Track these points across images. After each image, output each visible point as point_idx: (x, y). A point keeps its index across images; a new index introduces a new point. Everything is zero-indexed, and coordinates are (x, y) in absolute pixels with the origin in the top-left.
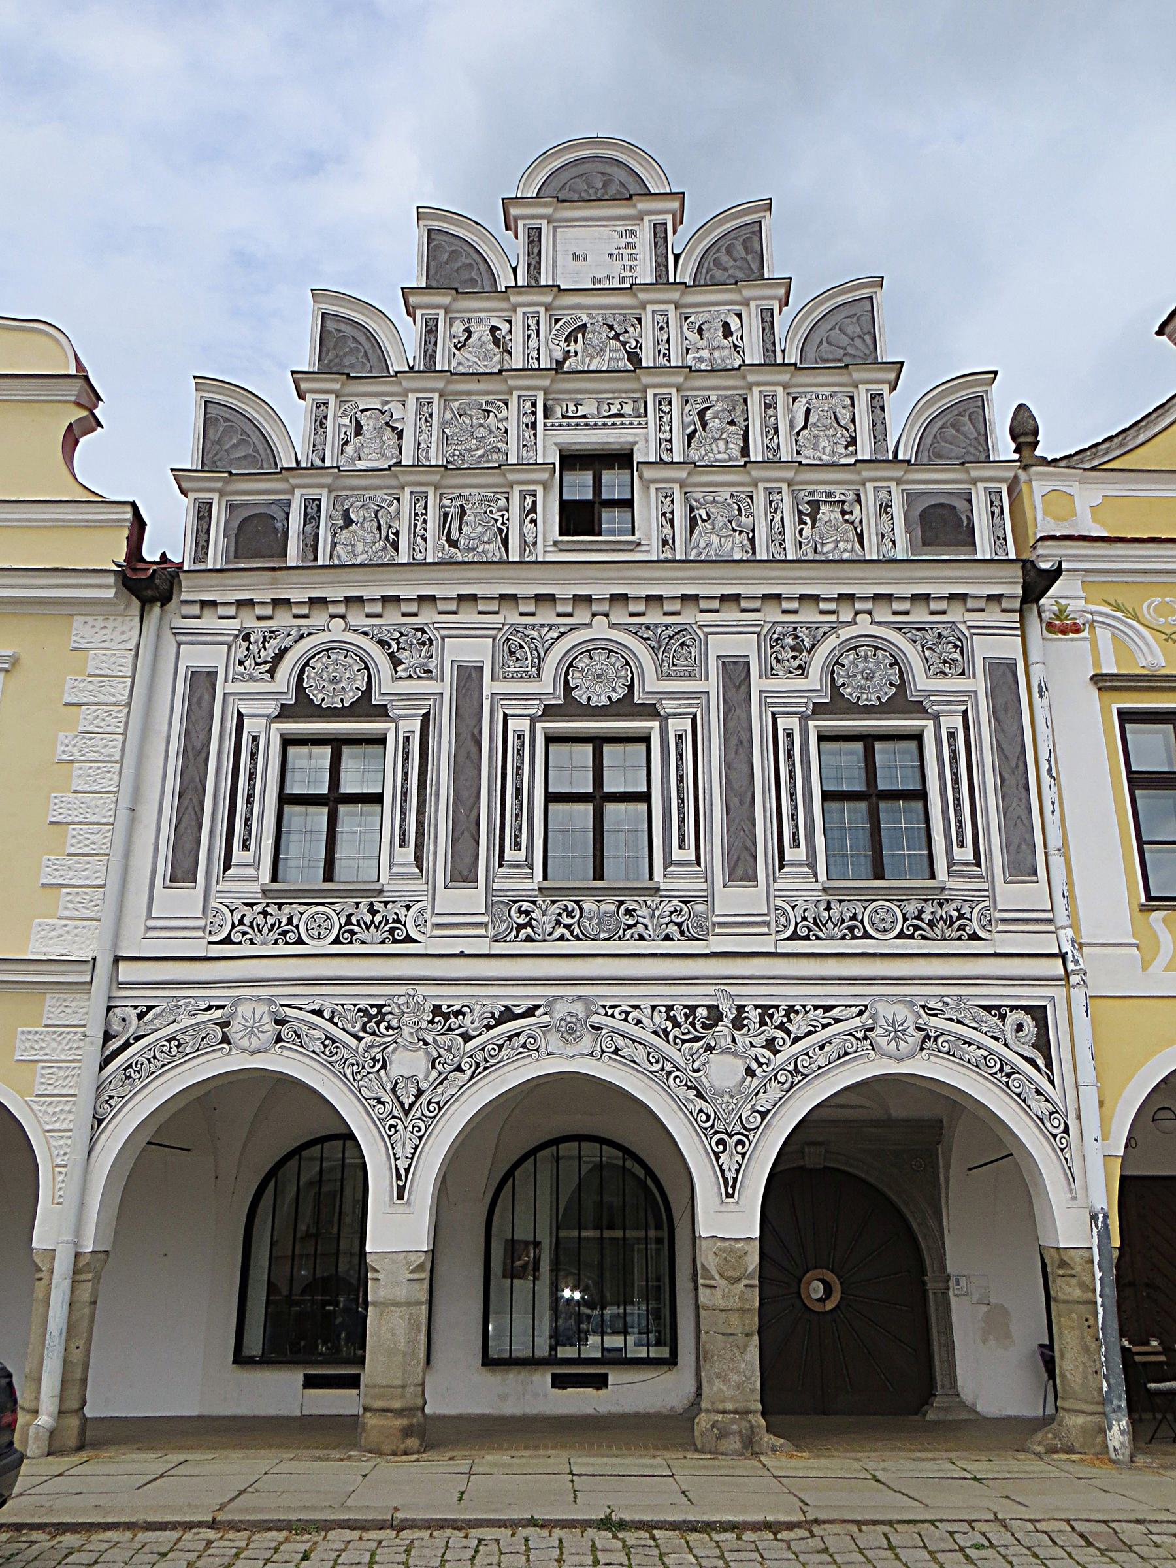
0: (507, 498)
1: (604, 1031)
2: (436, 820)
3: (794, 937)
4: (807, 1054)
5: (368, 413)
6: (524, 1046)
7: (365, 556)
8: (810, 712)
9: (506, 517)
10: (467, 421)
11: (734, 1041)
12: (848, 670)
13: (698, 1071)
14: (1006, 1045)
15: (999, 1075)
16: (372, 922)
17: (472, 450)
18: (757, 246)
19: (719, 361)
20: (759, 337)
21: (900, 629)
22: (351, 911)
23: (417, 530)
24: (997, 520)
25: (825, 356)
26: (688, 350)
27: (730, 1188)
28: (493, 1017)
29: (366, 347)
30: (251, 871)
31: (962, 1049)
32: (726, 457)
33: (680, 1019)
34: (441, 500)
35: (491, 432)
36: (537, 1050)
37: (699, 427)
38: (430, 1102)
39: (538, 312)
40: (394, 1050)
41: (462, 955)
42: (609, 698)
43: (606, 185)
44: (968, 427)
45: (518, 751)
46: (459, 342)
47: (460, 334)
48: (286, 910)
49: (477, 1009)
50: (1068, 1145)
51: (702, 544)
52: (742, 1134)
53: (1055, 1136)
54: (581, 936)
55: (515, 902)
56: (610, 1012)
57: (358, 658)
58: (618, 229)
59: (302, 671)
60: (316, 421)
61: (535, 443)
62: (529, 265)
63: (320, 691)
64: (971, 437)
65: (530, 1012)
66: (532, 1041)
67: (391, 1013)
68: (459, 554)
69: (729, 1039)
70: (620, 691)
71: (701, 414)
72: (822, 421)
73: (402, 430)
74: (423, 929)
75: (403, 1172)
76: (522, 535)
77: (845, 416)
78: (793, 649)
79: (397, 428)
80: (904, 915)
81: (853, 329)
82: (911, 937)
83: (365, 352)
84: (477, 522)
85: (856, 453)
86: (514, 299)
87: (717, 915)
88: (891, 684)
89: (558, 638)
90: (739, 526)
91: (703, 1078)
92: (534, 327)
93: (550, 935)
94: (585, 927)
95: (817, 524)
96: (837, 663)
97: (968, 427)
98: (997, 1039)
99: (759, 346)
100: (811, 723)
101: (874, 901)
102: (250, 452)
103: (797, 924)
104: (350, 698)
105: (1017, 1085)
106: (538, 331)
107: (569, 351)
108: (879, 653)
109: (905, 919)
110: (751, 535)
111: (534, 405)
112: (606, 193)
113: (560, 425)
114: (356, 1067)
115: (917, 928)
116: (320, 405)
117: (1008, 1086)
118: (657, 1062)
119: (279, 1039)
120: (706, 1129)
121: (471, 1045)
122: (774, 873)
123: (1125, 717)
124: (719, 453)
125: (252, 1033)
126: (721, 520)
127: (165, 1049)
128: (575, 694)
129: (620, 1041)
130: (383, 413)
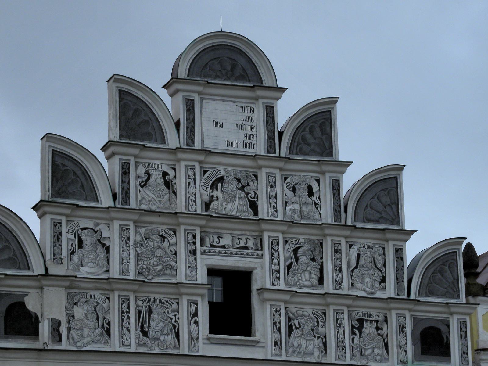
0: (178, 303)
5: (86, 231)
7: (89, 339)
9: (177, 317)
18: (328, 129)
19: (306, 213)
20: (331, 201)
23: (124, 323)
24: (464, 340)
26: (286, 203)
34: (136, 301)
35: (166, 253)
39: (194, 166)
43: (234, 67)
44: (448, 274)
46: (142, 182)
47: (143, 175)
51: (296, 344)
58: (243, 105)
60: (54, 236)
61: (196, 266)
62: (187, 128)
64: (450, 281)
68: (149, 342)
71: (295, 251)
72: (368, 264)
73: (109, 246)
76: (189, 332)
79: (105, 245)
81: (386, 199)
83: (82, 183)
84: (160, 319)
85: (385, 288)
86: (180, 155)
90: (317, 333)
95: (362, 335)
99: (331, 207)
102: (11, 255)
106: (194, 180)
107: (213, 196)
110: (324, 340)
111: (194, 237)
113: (209, 252)
116: (56, 224)
124: (306, 280)
126: (307, 329)
130: (96, 232)
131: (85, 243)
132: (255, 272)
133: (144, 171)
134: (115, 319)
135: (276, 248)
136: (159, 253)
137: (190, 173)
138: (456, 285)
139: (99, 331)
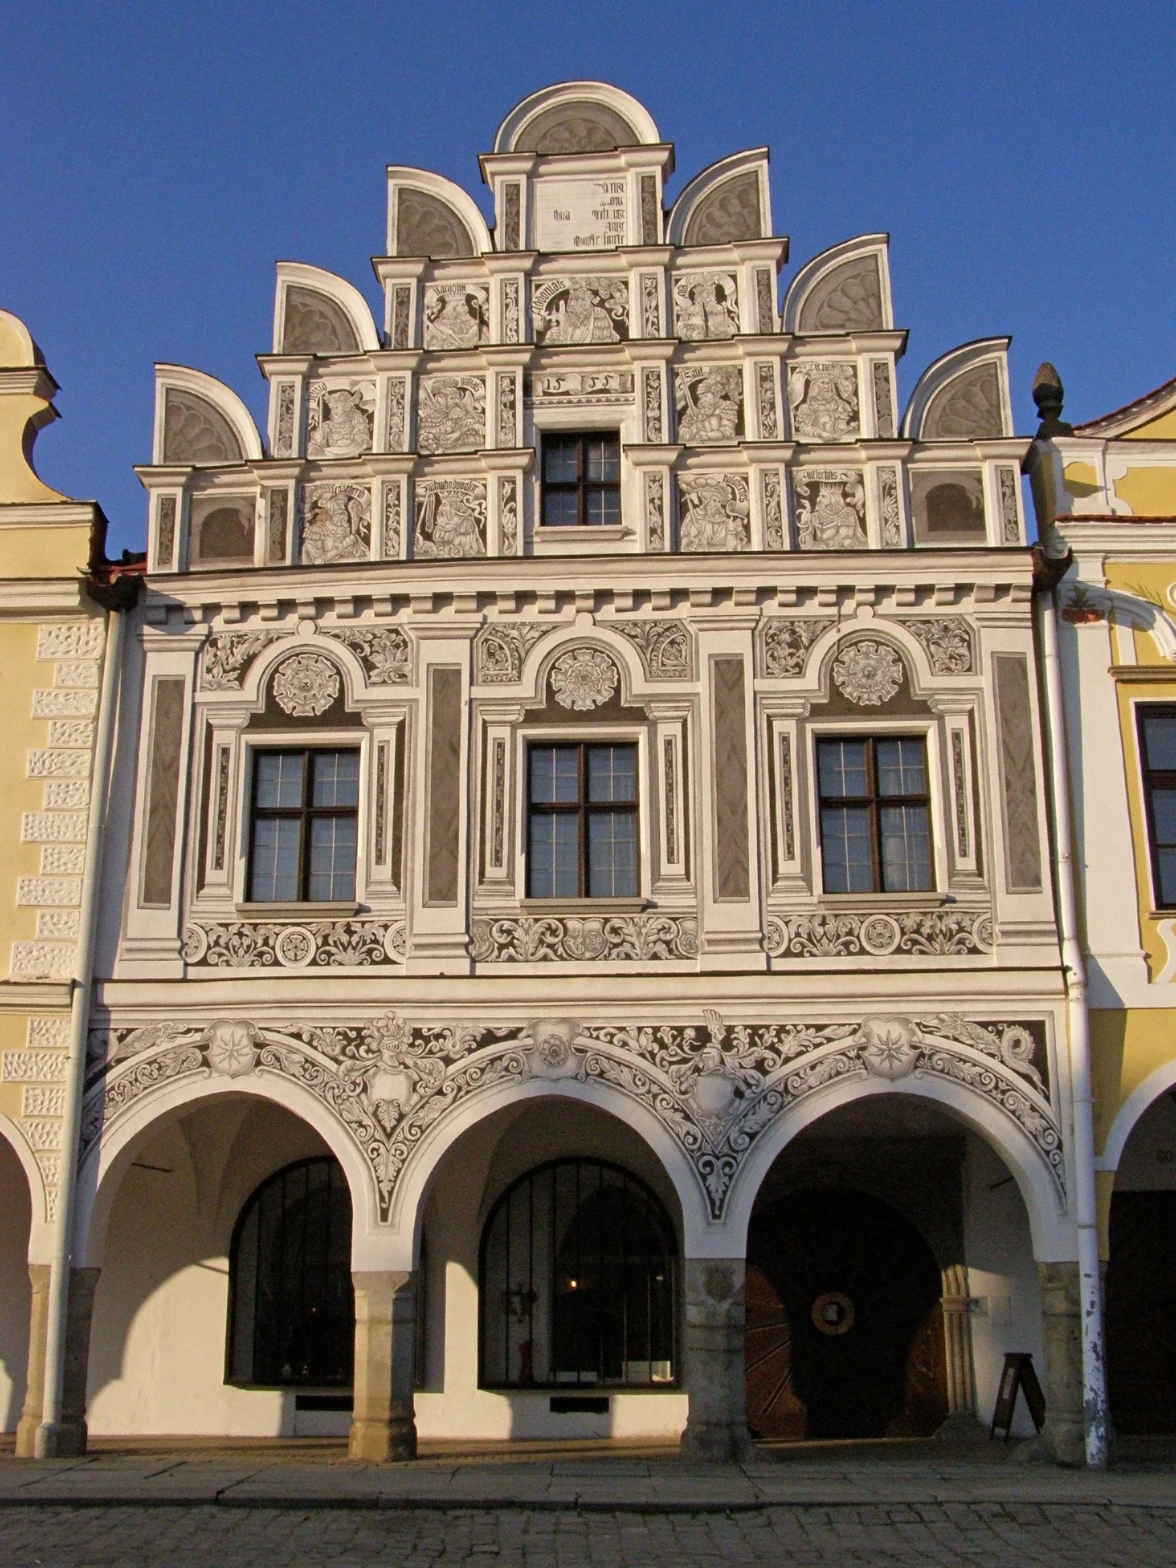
0: (485, 486)
1: (589, 1054)
2: (413, 836)
3: (788, 954)
4: (798, 1075)
6: (507, 1069)
7: (334, 552)
8: (807, 714)
9: (484, 506)
10: (442, 401)
11: (722, 1062)
12: (849, 667)
13: (683, 1093)
14: (1002, 1062)
15: (994, 1093)
16: (349, 943)
17: (446, 433)
18: (753, 198)
21: (904, 622)
22: (327, 932)
24: (1008, 502)
25: (826, 322)
27: (716, 1208)
28: (475, 1040)
29: (334, 322)
30: (224, 891)
31: (957, 1067)
32: (719, 435)
33: (668, 1040)
35: (467, 411)
36: (520, 1073)
37: (690, 402)
38: (411, 1126)
40: (375, 1074)
41: (442, 976)
42: (594, 701)
43: (591, 132)
44: (980, 398)
45: (499, 760)
48: (262, 931)
49: (459, 1033)
50: (1062, 1161)
51: (694, 532)
52: (729, 1156)
53: (1048, 1153)
54: (565, 955)
55: (496, 921)
56: (595, 1034)
57: (329, 663)
59: (272, 679)
62: (507, 226)
63: (291, 700)
64: (983, 409)
65: (513, 1035)
66: (515, 1064)
67: (370, 1036)
69: (717, 1060)
70: (605, 693)
73: (373, 413)
74: (401, 950)
75: (386, 1195)
76: (501, 527)
77: (846, 387)
78: (790, 645)
80: (902, 929)
81: (857, 291)
82: (909, 952)
87: (707, 933)
88: (894, 682)
89: (540, 636)
90: (733, 511)
91: (691, 1101)
92: (512, 295)
93: (532, 955)
94: (569, 946)
95: (817, 508)
96: (837, 660)
97: (980, 398)
98: (992, 1055)
100: (809, 727)
101: (871, 914)
103: (790, 940)
104: (323, 705)
105: (1011, 1102)
106: (517, 300)
107: (550, 321)
108: (882, 649)
109: (903, 933)
110: (745, 522)
111: (513, 382)
112: (590, 142)
114: (336, 1091)
115: (915, 942)
117: (1002, 1103)
118: (644, 1084)
119: (258, 1063)
120: (692, 1151)
121: (453, 1068)
122: (767, 886)
123: (1145, 712)
124: (712, 430)
125: (231, 1056)
126: (713, 506)
127: (146, 1071)
128: (558, 698)
129: (605, 1064)
131: (333, 412)
132: (622, 427)
133: (436, 297)
134: (375, 518)
135: (656, 385)
136: (456, 413)
137: (510, 290)
138: (994, 414)
139: (350, 540)
